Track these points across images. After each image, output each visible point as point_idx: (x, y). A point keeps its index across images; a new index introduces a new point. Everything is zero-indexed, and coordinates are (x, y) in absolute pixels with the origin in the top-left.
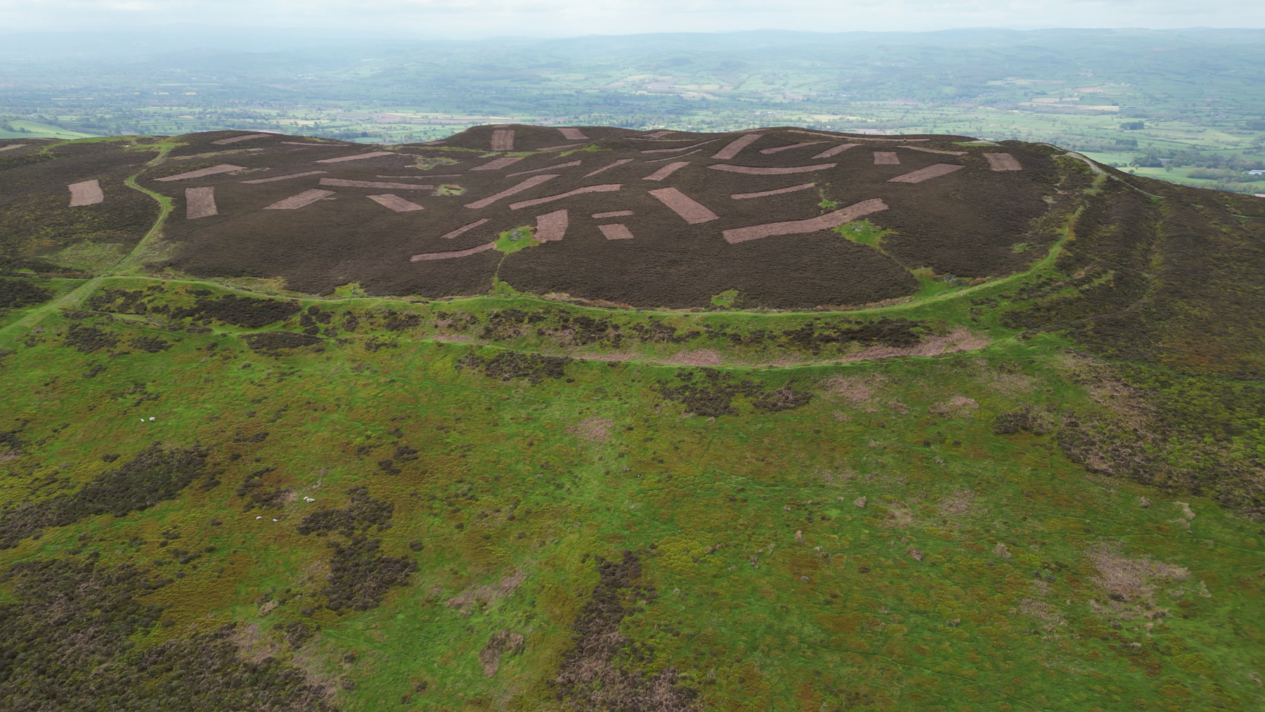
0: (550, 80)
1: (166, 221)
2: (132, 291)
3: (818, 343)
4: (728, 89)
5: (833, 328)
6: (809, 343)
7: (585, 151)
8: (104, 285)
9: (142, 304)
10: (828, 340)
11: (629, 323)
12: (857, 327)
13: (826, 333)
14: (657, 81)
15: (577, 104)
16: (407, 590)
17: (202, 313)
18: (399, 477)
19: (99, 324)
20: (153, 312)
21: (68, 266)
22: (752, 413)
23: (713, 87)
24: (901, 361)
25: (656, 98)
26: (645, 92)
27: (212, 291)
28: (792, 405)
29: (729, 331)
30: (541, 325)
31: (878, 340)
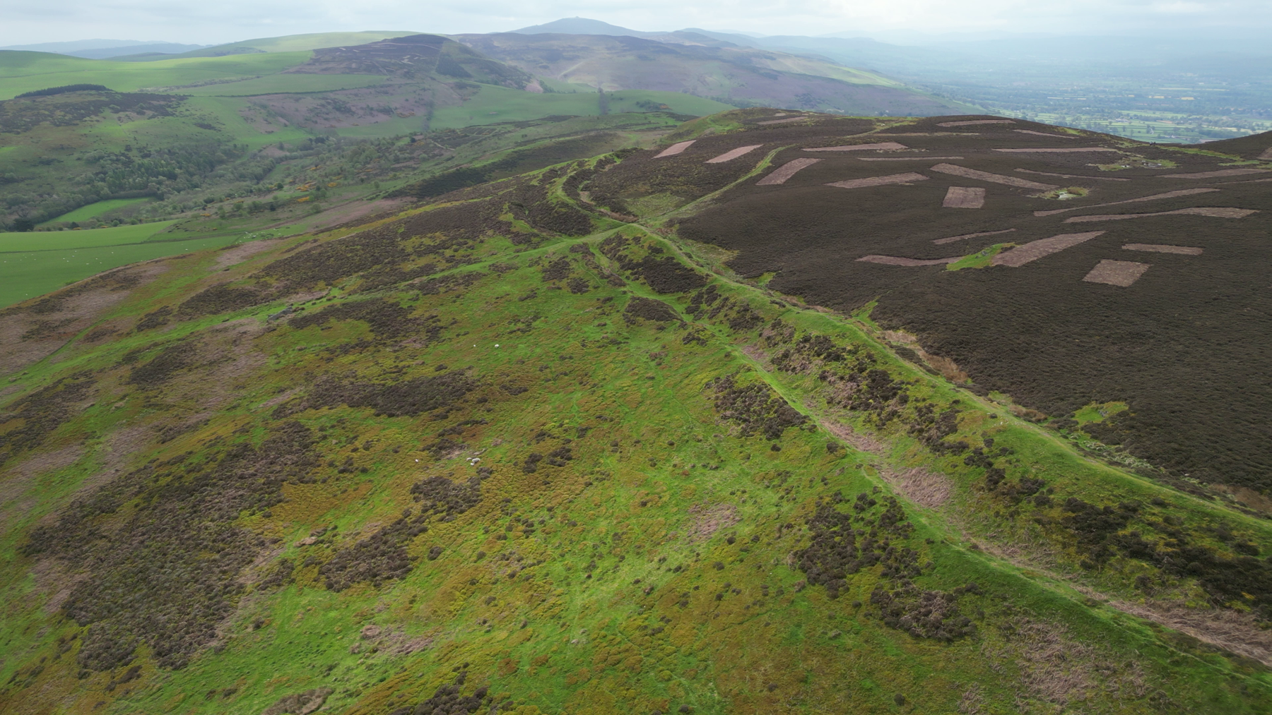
1: (737, 185)
3: (1113, 548)
5: (1171, 535)
6: (1093, 542)
10: (1140, 551)
11: (924, 400)
12: (1227, 553)
13: (1148, 538)
16: (372, 591)
18: (525, 477)
22: (858, 605)
24: (1227, 666)
28: (922, 631)
29: (1000, 463)
30: (833, 366)
31: (1255, 604)
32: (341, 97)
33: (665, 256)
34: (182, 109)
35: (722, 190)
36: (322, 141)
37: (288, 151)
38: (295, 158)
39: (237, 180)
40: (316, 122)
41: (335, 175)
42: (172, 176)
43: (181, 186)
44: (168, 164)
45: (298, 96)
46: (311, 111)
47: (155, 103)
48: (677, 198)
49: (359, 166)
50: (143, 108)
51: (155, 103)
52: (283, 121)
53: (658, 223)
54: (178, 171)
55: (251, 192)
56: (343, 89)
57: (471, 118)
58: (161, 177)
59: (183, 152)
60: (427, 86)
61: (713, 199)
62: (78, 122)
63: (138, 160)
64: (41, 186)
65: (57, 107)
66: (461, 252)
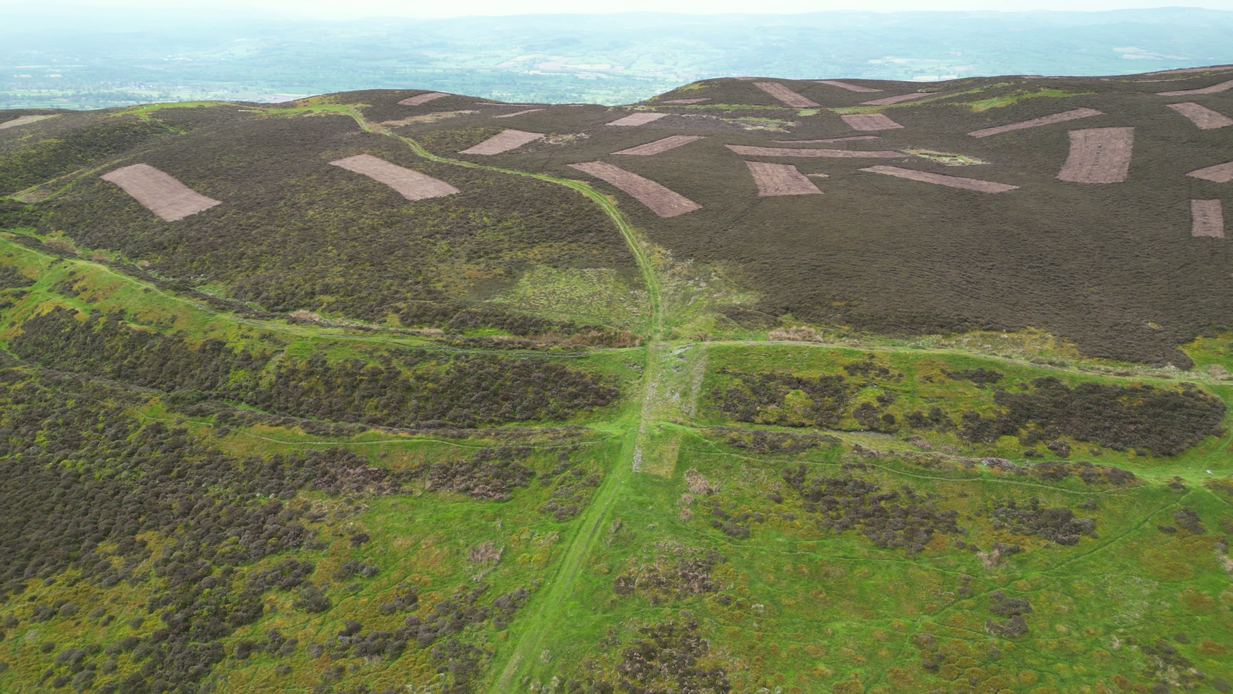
0: (438, 60)
2: (814, 374)
4: (620, 70)
7: (616, 127)
8: (723, 363)
9: (866, 406)
14: (548, 61)
15: (474, 84)
17: (1031, 425)
19: (852, 467)
20: (913, 426)
21: (566, 318)
23: (605, 67)
25: (551, 77)
26: (538, 72)
27: (998, 371)
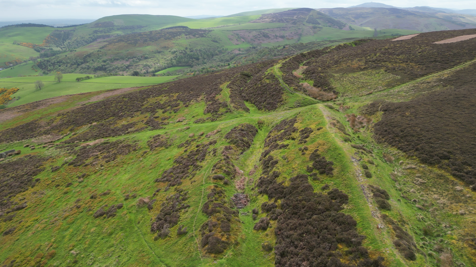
32: (266, 31)
33: (332, 184)
34: (209, 35)
35: (453, 69)
36: (254, 48)
37: (242, 51)
38: (243, 54)
39: (220, 62)
40: (255, 41)
41: (250, 61)
42: (198, 59)
43: (200, 63)
44: (198, 54)
45: (250, 31)
46: (254, 36)
47: (200, 32)
48: (391, 76)
49: (260, 57)
50: (195, 34)
51: (200, 32)
52: (243, 40)
53: (357, 105)
54: (200, 57)
55: (219, 66)
56: (268, 28)
57: (316, 40)
58: (194, 59)
59: (204, 50)
60: (300, 27)
61: (440, 80)
62: (172, 38)
63: (188, 53)
64: (155, 60)
65: (168, 33)
66: (166, 115)
